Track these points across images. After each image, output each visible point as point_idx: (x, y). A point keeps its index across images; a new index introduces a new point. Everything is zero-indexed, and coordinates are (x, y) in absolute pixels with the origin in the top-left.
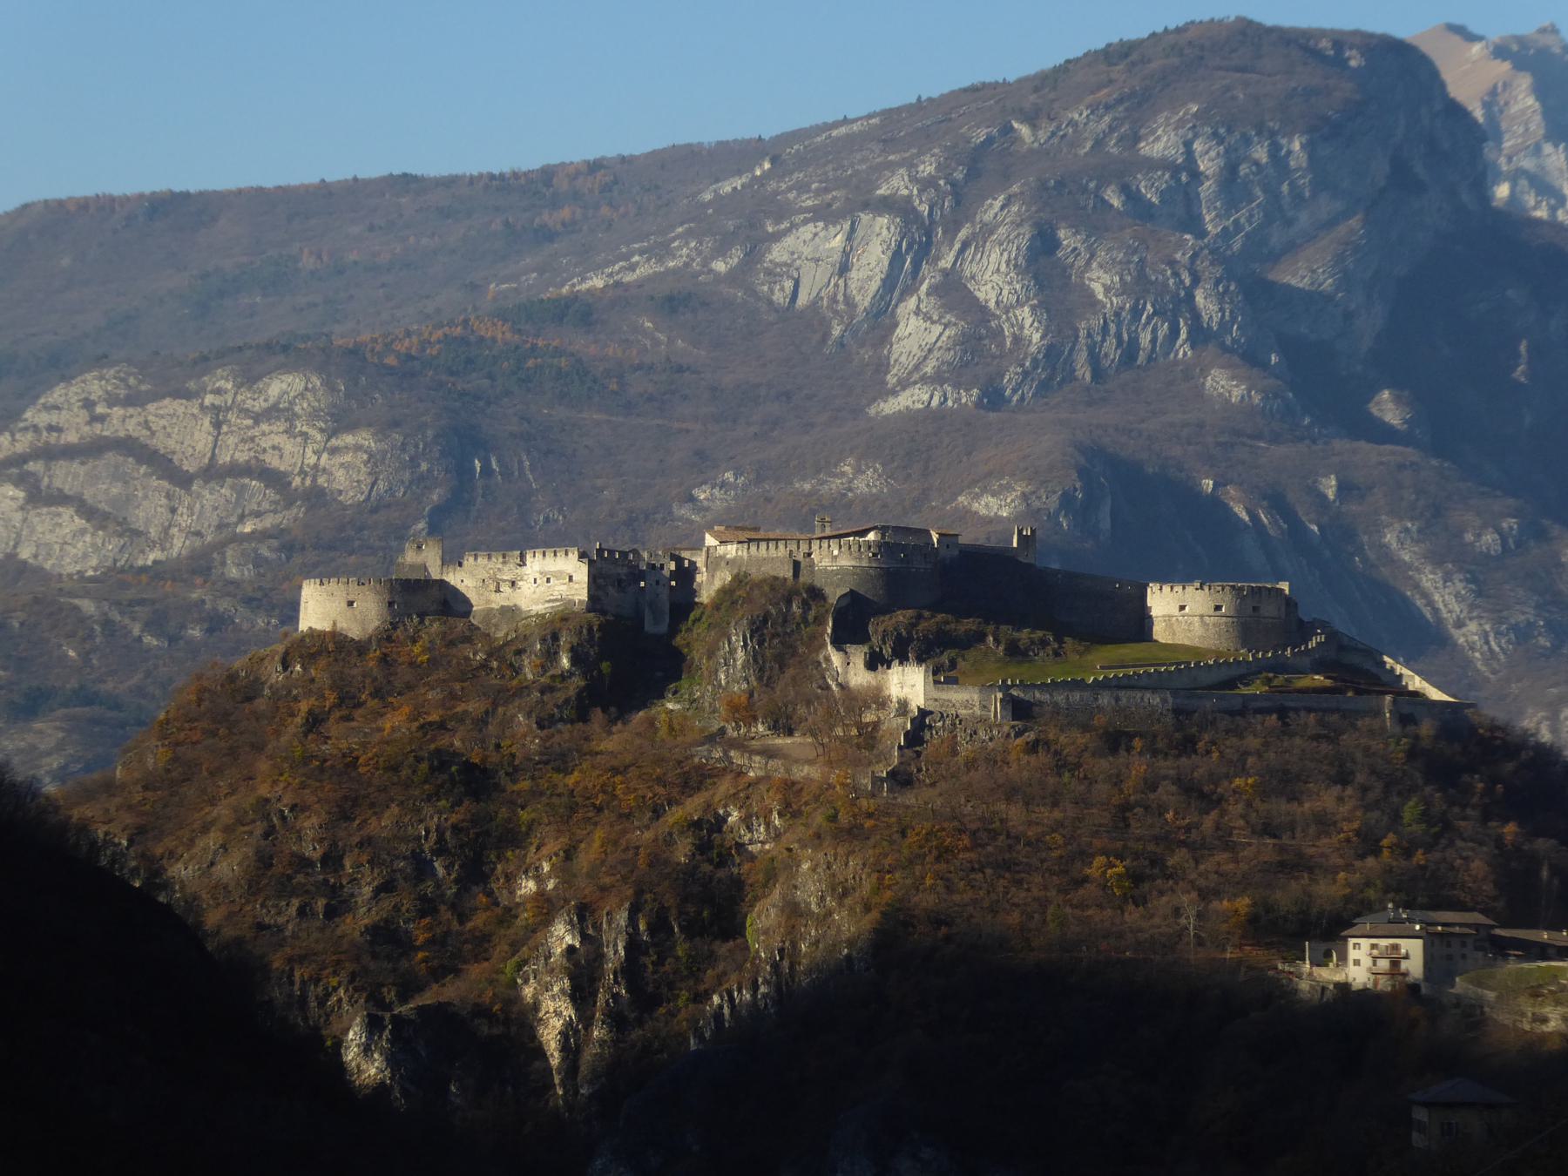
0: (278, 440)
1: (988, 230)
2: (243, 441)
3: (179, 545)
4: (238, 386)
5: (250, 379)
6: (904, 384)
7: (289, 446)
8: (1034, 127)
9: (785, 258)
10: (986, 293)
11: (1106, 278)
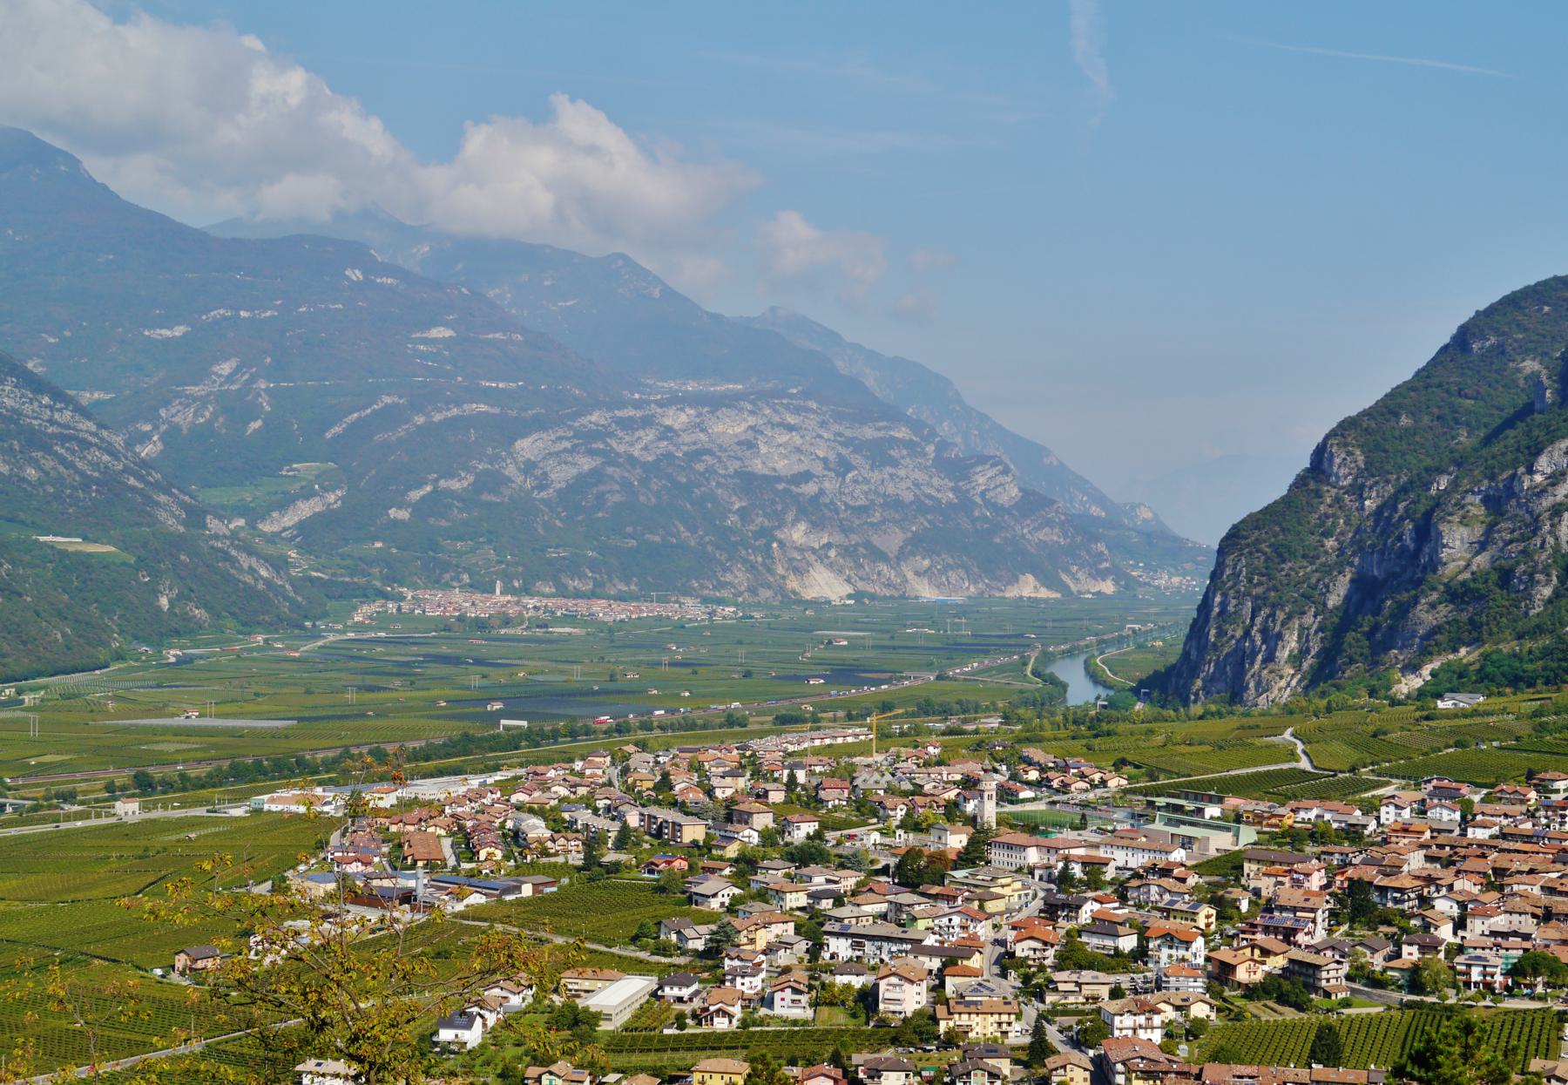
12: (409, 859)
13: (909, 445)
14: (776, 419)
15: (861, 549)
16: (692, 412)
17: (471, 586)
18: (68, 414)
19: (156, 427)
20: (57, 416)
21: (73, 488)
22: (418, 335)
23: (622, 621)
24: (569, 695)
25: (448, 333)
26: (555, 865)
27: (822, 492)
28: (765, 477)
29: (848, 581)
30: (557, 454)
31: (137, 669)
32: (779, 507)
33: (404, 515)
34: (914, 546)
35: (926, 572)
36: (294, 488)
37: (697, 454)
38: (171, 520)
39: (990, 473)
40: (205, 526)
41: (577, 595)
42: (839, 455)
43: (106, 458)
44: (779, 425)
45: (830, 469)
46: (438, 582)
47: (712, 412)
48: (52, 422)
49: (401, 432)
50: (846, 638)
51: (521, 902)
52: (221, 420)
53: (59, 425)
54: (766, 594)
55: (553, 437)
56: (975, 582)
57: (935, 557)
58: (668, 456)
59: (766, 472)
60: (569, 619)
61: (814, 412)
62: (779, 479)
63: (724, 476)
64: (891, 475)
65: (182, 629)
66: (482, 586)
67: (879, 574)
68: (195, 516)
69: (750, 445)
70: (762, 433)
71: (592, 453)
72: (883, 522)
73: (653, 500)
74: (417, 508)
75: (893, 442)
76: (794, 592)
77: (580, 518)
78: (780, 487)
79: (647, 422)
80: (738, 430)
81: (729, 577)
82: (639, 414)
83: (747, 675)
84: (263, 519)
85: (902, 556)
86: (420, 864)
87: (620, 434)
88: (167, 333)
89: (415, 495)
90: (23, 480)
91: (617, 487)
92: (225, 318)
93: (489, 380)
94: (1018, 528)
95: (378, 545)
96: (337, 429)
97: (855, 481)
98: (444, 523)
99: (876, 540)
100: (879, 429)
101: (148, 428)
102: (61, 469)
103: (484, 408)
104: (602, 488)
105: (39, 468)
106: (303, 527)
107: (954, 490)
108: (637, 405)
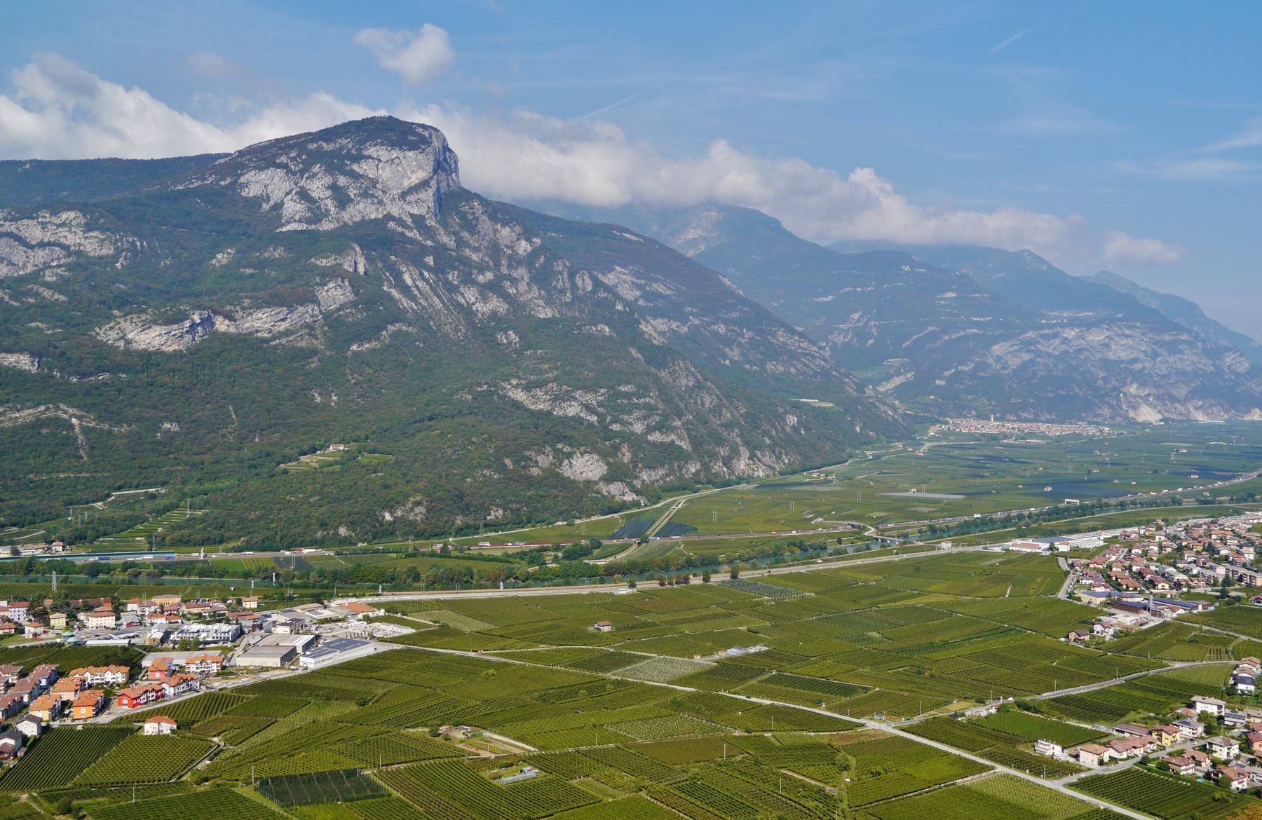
0: (67, 234)
1: (315, 175)
2: (53, 234)
3: (30, 269)
4: (51, 215)
5: (55, 213)
6: (288, 222)
7: (69, 236)
8: (328, 144)
9: (246, 181)
10: (315, 195)
11: (355, 192)
12: (1124, 587)
13: (1189, 343)
14: (1120, 332)
15: (1166, 397)
16: (1077, 330)
17: (977, 416)
18: (806, 344)
19: (827, 344)
20: (801, 345)
21: (810, 376)
22: (940, 296)
23: (1059, 436)
24: (1078, 482)
25: (954, 295)
26: (1199, 594)
27: (1144, 368)
28: (1115, 361)
29: (1160, 412)
30: (1012, 352)
31: (859, 462)
32: (1123, 376)
33: (943, 383)
34: (1194, 394)
35: (1200, 407)
36: (891, 371)
37: (1081, 350)
38: (851, 390)
39: (1232, 357)
40: (865, 393)
41: (1026, 420)
42: (1153, 349)
43: (823, 363)
44: (1121, 335)
45: (1147, 356)
46: (961, 414)
47: (1088, 330)
48: (800, 347)
49: (939, 343)
50: (1186, 448)
51: (1200, 614)
52: (855, 340)
53: (803, 349)
54: (1119, 419)
55: (1010, 344)
56: (1227, 412)
57: (1205, 400)
58: (1066, 352)
59: (1115, 358)
60: (1032, 435)
61: (1139, 328)
62: (1122, 362)
63: (1094, 361)
64: (1180, 359)
65: (865, 442)
66: (983, 417)
67: (1175, 408)
68: (860, 387)
69: (1107, 346)
70: (1112, 339)
71: (1029, 351)
72: (1177, 382)
73: (1060, 374)
74: (948, 379)
75: (1181, 341)
76: (1132, 418)
77: (1025, 383)
78: (1123, 366)
79: (1056, 335)
80: (1100, 338)
81: (1100, 412)
82: (1051, 332)
83: (1155, 472)
84: (878, 385)
85: (1187, 399)
86: (1131, 589)
87: (1042, 341)
88: (825, 299)
89: (947, 374)
90: (790, 373)
91: (1042, 368)
92: (850, 291)
93: (975, 317)
94: (1249, 384)
95: (932, 397)
96: (908, 343)
97: (1161, 362)
98: (961, 387)
99: (1174, 392)
100: (1173, 335)
101: (824, 344)
102: (805, 368)
103: (975, 331)
104: (1035, 368)
105: (796, 368)
106: (896, 389)
107: (1214, 365)
108: (1050, 327)
